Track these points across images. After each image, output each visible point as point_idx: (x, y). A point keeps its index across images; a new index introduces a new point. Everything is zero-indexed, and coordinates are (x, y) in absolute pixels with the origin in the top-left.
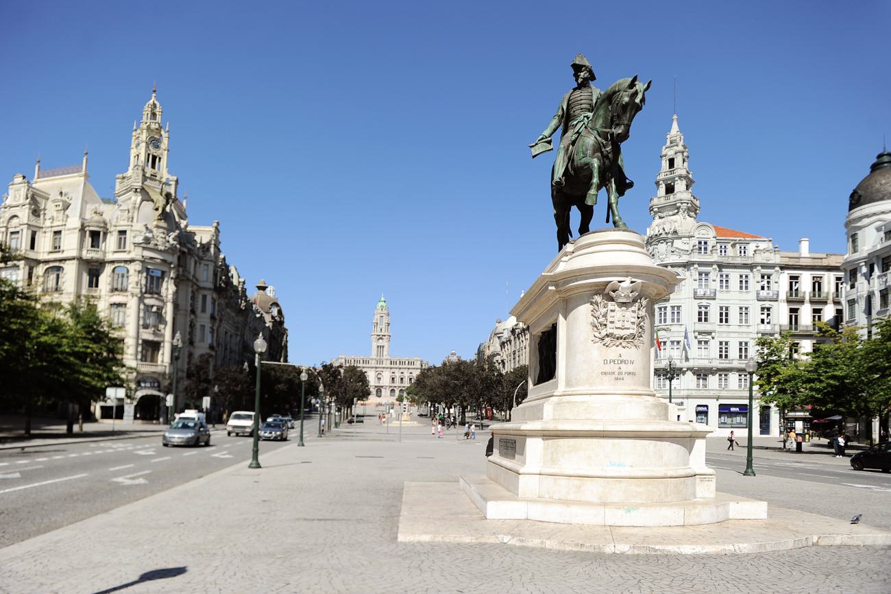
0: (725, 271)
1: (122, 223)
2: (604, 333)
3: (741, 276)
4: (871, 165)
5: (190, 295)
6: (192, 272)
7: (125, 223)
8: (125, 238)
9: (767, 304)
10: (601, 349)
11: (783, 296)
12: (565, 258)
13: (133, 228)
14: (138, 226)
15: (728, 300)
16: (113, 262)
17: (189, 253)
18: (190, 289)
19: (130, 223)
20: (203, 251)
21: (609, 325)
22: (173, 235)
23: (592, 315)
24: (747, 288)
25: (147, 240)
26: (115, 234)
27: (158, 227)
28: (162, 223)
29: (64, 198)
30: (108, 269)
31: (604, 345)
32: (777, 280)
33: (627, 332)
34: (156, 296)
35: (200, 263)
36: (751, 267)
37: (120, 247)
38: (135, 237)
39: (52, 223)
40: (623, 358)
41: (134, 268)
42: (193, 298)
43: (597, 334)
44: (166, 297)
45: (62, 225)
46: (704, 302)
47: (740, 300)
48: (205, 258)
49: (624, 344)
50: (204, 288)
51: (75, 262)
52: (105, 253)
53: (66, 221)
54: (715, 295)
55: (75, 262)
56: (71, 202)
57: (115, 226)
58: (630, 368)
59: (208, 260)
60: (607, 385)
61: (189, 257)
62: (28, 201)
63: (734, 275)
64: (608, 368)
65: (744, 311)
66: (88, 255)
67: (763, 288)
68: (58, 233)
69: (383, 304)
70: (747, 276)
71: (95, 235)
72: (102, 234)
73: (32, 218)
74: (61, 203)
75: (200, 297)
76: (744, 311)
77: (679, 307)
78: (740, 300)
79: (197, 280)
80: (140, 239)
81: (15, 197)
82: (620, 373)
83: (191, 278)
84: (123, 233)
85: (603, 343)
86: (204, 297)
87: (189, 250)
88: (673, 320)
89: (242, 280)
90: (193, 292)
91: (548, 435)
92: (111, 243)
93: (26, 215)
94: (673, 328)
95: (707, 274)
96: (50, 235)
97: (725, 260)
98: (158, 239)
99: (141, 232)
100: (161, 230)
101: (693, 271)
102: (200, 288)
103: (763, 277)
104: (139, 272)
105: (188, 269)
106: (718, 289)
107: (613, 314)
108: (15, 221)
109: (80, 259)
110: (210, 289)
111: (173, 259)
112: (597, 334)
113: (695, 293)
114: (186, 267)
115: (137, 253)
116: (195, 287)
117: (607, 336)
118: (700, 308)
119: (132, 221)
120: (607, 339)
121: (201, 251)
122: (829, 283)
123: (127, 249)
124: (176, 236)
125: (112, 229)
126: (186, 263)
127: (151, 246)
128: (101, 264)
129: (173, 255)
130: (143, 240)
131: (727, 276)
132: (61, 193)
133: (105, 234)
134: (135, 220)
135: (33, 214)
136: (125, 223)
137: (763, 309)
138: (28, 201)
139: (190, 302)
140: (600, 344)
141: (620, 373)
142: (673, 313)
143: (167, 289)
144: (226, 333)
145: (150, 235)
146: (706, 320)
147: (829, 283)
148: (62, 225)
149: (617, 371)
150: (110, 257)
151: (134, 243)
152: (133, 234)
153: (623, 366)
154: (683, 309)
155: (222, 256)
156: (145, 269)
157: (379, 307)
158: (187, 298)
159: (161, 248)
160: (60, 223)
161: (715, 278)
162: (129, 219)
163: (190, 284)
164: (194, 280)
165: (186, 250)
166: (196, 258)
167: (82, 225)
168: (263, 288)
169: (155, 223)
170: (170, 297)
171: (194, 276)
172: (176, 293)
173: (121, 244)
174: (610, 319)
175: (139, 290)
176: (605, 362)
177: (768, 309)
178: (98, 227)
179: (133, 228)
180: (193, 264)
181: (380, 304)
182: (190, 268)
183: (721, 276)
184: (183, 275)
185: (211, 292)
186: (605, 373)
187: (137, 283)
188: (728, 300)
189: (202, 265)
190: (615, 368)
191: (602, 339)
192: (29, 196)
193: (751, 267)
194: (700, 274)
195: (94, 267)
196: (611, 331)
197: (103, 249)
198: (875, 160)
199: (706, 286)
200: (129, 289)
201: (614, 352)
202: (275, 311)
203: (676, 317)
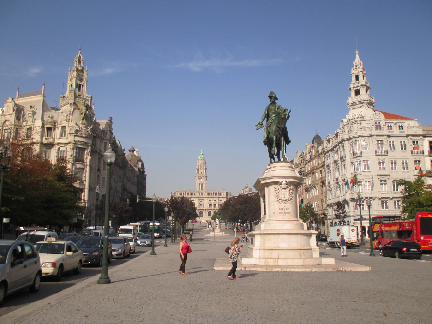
0: (392, 139)
1: (63, 122)
3: (401, 142)
5: (97, 160)
6: (99, 148)
8: (65, 131)
9: (417, 158)
11: (426, 153)
12: (266, 171)
13: (70, 125)
14: (72, 124)
15: (395, 156)
16: (58, 144)
18: (97, 157)
19: (68, 123)
20: (104, 135)
21: (280, 196)
22: (89, 128)
24: (405, 149)
25: (77, 131)
26: (60, 128)
27: (82, 124)
28: (85, 122)
29: (32, 109)
30: (55, 148)
32: (422, 144)
33: (287, 198)
34: (81, 163)
35: (102, 142)
36: (407, 136)
37: (62, 136)
38: (71, 130)
39: (26, 123)
40: (286, 207)
41: (71, 146)
42: (99, 162)
44: (86, 162)
46: (381, 158)
47: (402, 156)
51: (39, 145)
52: (54, 139)
53: (34, 122)
54: (387, 153)
55: (39, 145)
56: (36, 111)
57: (60, 124)
58: (288, 211)
60: (280, 217)
62: (15, 112)
63: (397, 142)
64: (281, 211)
65: (405, 163)
66: (46, 141)
67: (414, 149)
69: (202, 156)
70: (404, 142)
71: (49, 129)
73: (16, 121)
74: (31, 112)
76: (405, 163)
77: (367, 161)
78: (402, 156)
79: (101, 151)
80: (73, 131)
81: (8, 110)
82: (285, 213)
83: (98, 151)
84: (64, 128)
87: (97, 134)
88: (365, 169)
89: (123, 149)
90: (99, 159)
91: (261, 234)
92: (57, 133)
93: (13, 120)
94: (366, 174)
95: (381, 141)
97: (391, 134)
99: (73, 127)
100: (84, 126)
101: (374, 140)
103: (414, 142)
104: (72, 149)
106: (389, 150)
107: (281, 192)
108: (7, 123)
109: (41, 143)
111: (90, 142)
113: (376, 152)
114: (95, 145)
115: (71, 139)
116: (100, 156)
118: (380, 161)
119: (69, 122)
120: (280, 201)
121: (103, 135)
123: (66, 137)
124: (91, 128)
125: (59, 126)
127: (78, 134)
131: (393, 142)
132: (31, 107)
133: (54, 129)
134: (70, 121)
135: (17, 119)
136: (65, 122)
137: (415, 161)
138: (15, 112)
139: (97, 164)
140: (277, 203)
141: (285, 213)
142: (365, 165)
143: (87, 158)
145: (78, 129)
146: (384, 168)
149: (284, 212)
150: (57, 141)
151: (70, 134)
152: (69, 129)
153: (286, 210)
154: (369, 162)
155: (113, 136)
156: (75, 148)
157: (199, 158)
159: (84, 135)
160: (31, 123)
161: (386, 143)
162: (67, 120)
163: (97, 154)
164: (100, 152)
165: (95, 135)
167: (43, 124)
168: (133, 151)
169: (81, 122)
170: (88, 162)
171: (99, 150)
172: (91, 161)
173: (63, 135)
175: (72, 160)
176: (280, 209)
177: (419, 161)
178: (51, 125)
179: (70, 125)
180: (99, 142)
181: (200, 156)
183: (390, 142)
184: (94, 150)
186: (280, 213)
187: (71, 156)
188: (395, 156)
189: (103, 143)
190: (283, 211)
192: (15, 109)
193: (407, 136)
194: (378, 141)
196: (280, 198)
197: (54, 137)
199: (382, 149)
201: (283, 205)
202: (140, 164)
203: (366, 167)
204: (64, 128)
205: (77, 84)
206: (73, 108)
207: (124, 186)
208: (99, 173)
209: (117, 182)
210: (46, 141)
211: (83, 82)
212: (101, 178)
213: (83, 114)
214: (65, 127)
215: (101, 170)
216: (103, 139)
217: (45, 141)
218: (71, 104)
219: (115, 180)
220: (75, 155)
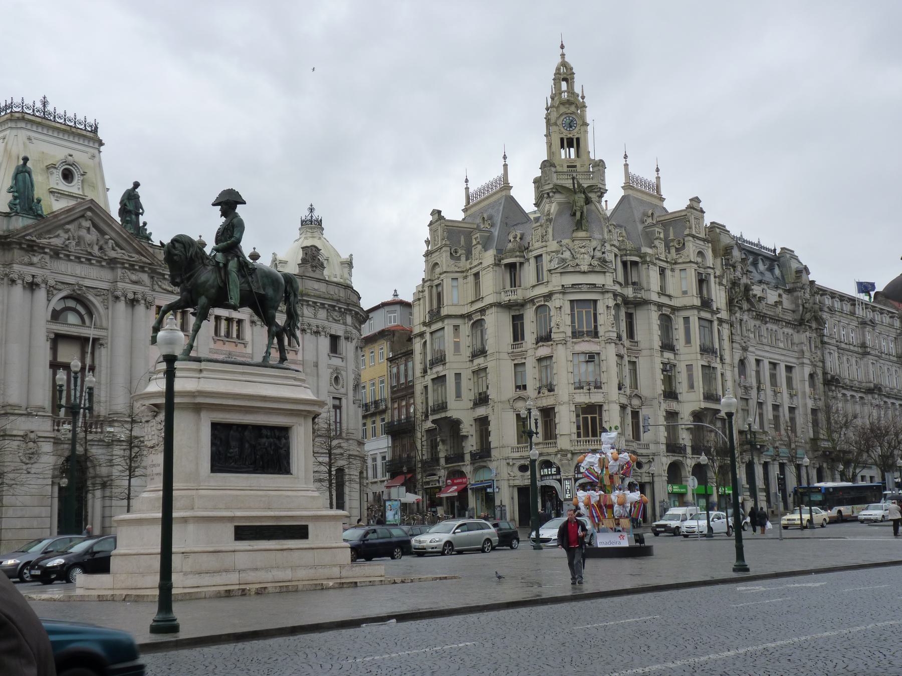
7: (539, 244)
13: (549, 250)
17: (645, 262)
19: (544, 244)
26: (532, 261)
34: (587, 339)
45: (479, 264)
48: (680, 261)
50: (685, 308)
55: (494, 309)
57: (531, 251)
59: (684, 263)
61: (646, 266)
68: (477, 275)
71: (512, 267)
72: (518, 264)
75: (681, 321)
79: (670, 296)
80: (554, 264)
83: (654, 297)
84: (538, 258)
86: (687, 320)
92: (528, 274)
96: (471, 279)
98: (578, 256)
99: (557, 252)
102: (675, 309)
105: (645, 285)
110: (693, 307)
126: (639, 276)
128: (522, 305)
129: (605, 272)
130: (558, 263)
134: (550, 236)
136: (539, 244)
144: (758, 362)
145: (567, 255)
148: (479, 264)
152: (549, 258)
158: (650, 329)
159: (585, 268)
163: (653, 308)
164: (664, 300)
166: (664, 264)
178: (511, 257)
182: (648, 283)
185: (696, 312)
189: (677, 272)
195: (517, 313)
200: (553, 336)
204: (538, 258)
205: (562, 140)
206: (554, 205)
207: (825, 373)
208: (668, 355)
209: (789, 369)
210: (507, 299)
211: (577, 129)
212: (682, 367)
213: (578, 214)
214: (541, 255)
215: (680, 344)
216: (676, 263)
217: (505, 298)
218: (548, 194)
219: (774, 365)
220: (569, 322)
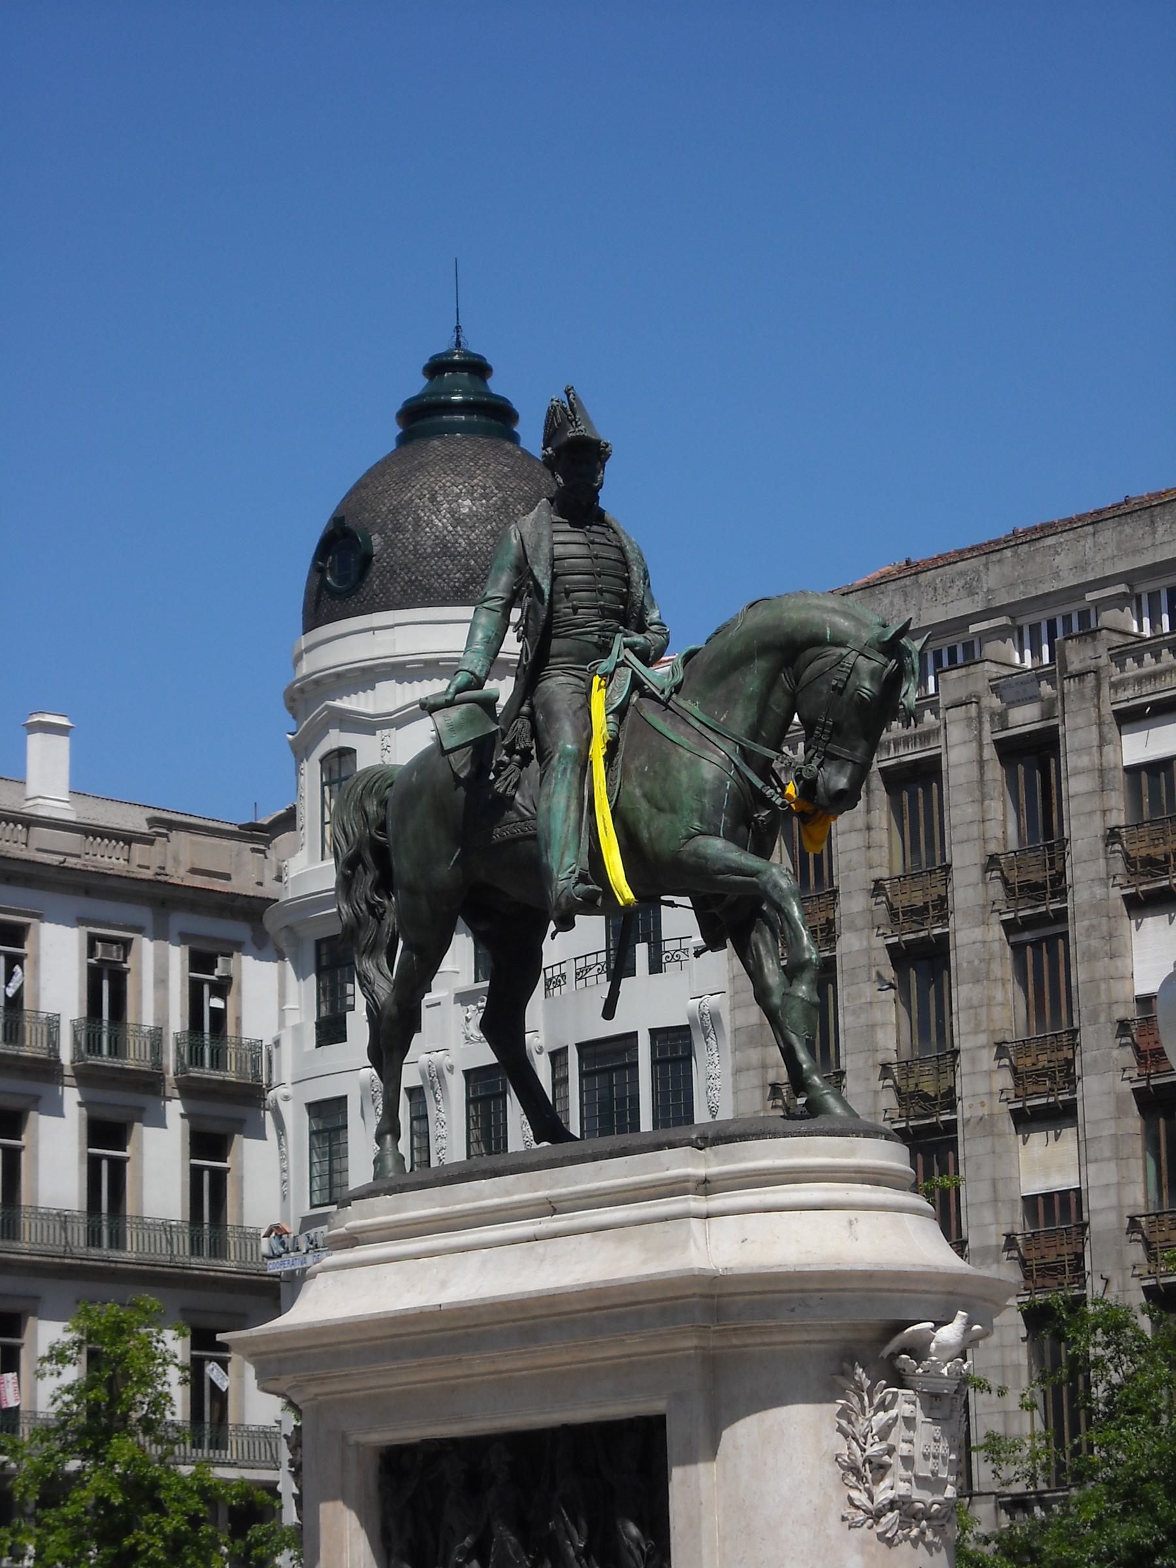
2: (884, 1493)
4: (399, 407)
10: (873, 1549)
23: (840, 1429)
31: (881, 1536)
43: (860, 1497)
49: (929, 1535)
85: (880, 1530)
112: (860, 1497)
117: (892, 1505)
122: (161, 982)
147: (161, 982)
174: (904, 1449)
191: (876, 1516)
196: (903, 1488)
198: (416, 385)
